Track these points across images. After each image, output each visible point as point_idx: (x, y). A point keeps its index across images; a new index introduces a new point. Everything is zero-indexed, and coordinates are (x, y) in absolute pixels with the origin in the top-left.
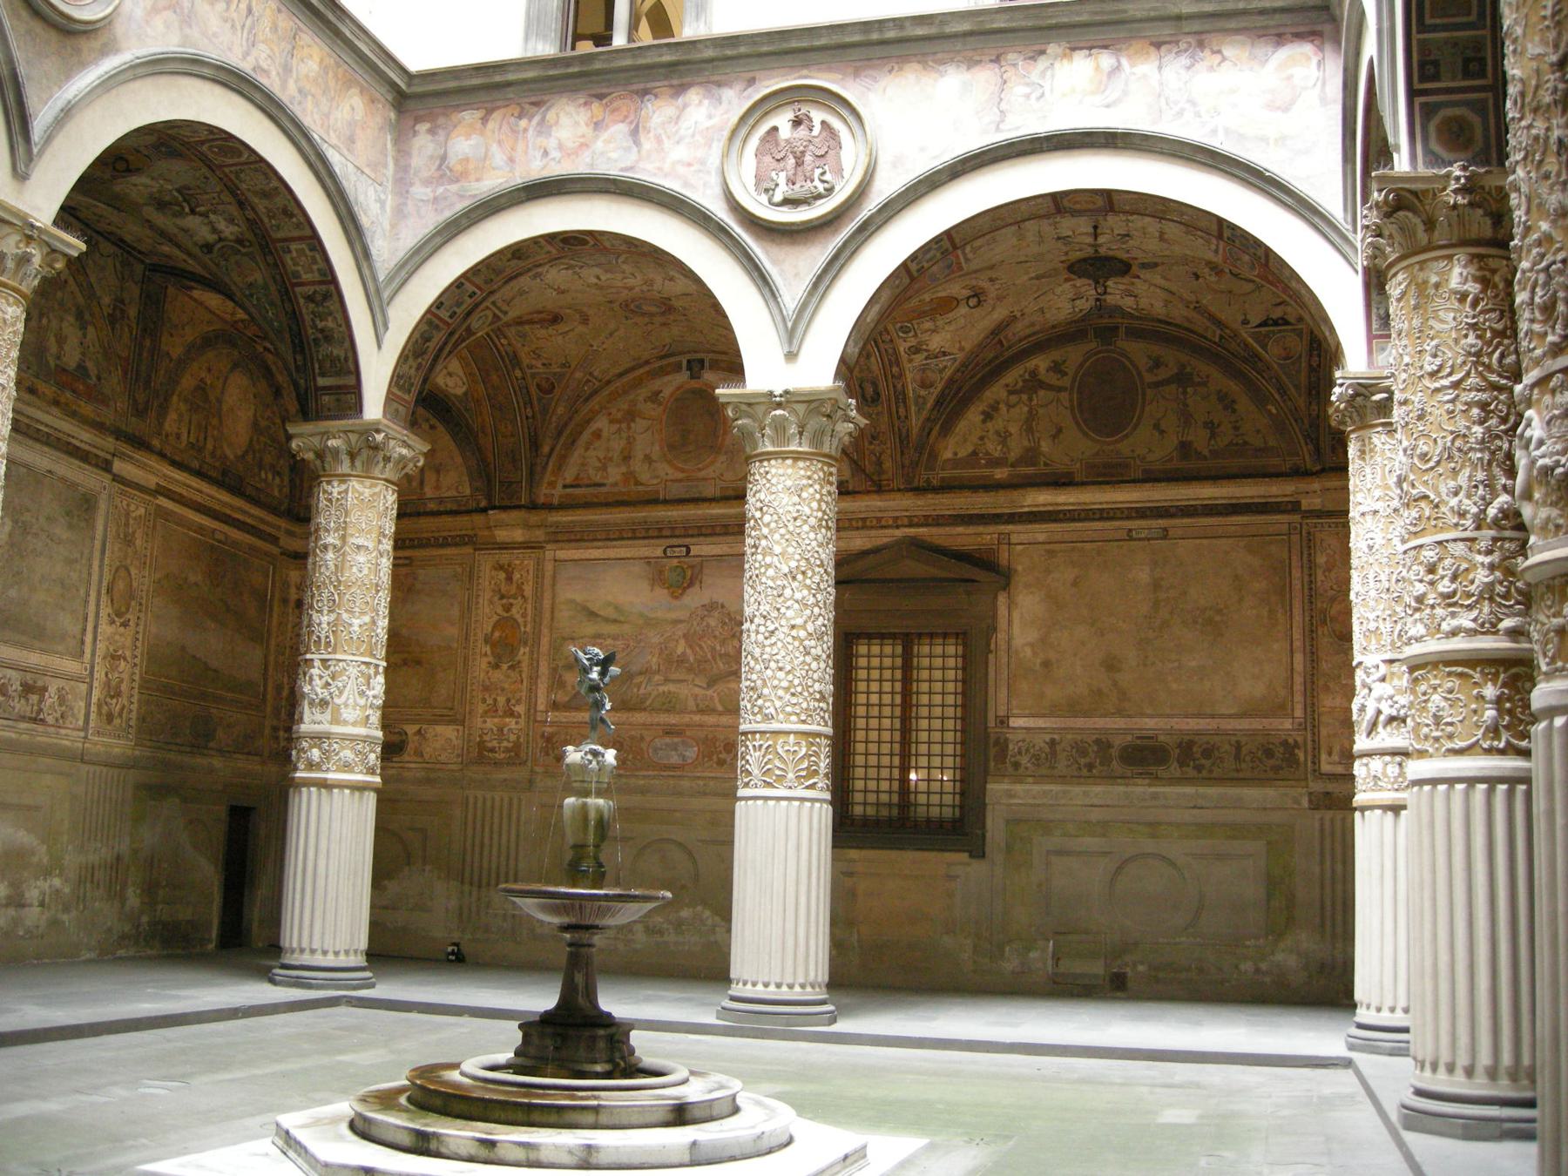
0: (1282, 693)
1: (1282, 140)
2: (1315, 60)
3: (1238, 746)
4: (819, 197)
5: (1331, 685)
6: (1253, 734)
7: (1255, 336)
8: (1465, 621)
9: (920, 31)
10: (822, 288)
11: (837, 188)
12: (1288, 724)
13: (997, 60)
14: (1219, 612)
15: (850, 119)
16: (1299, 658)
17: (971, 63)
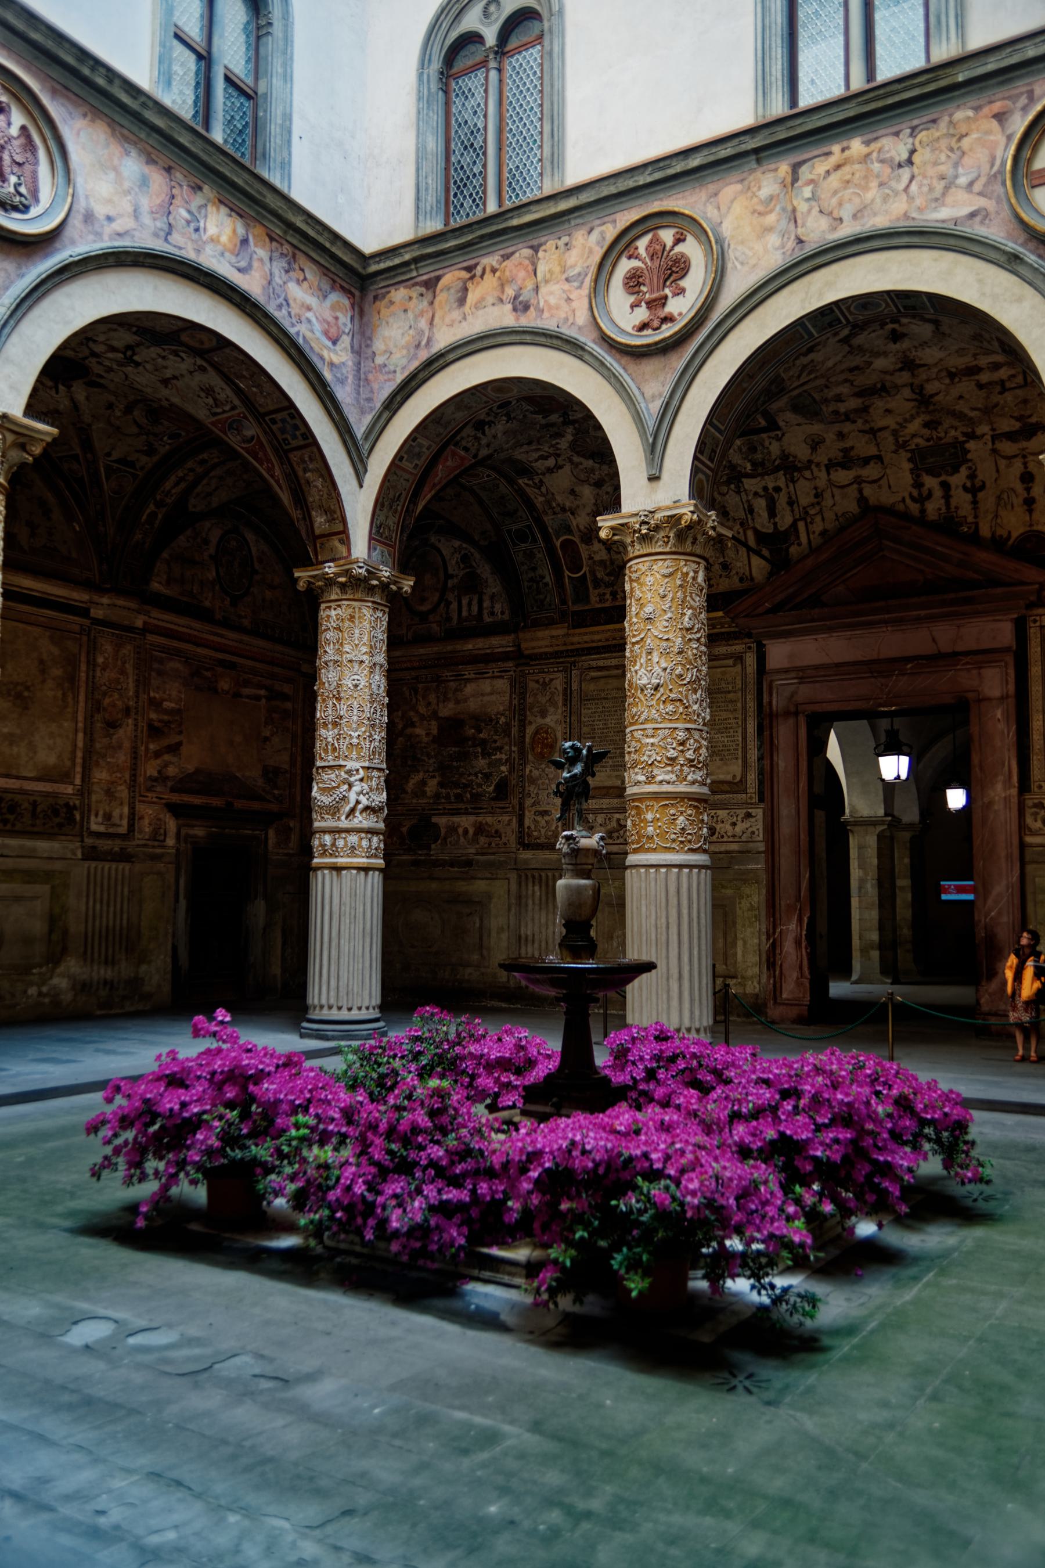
0: (68, 763)
1: (332, 364)
2: (349, 315)
3: (35, 804)
4: (15, 208)
5: (101, 761)
6: (47, 795)
8: (698, 776)
9: (125, 98)
10: (19, 313)
11: (34, 212)
12: (70, 790)
13: (168, 170)
14: (27, 688)
15: (52, 143)
16: (80, 736)
17: (151, 161)
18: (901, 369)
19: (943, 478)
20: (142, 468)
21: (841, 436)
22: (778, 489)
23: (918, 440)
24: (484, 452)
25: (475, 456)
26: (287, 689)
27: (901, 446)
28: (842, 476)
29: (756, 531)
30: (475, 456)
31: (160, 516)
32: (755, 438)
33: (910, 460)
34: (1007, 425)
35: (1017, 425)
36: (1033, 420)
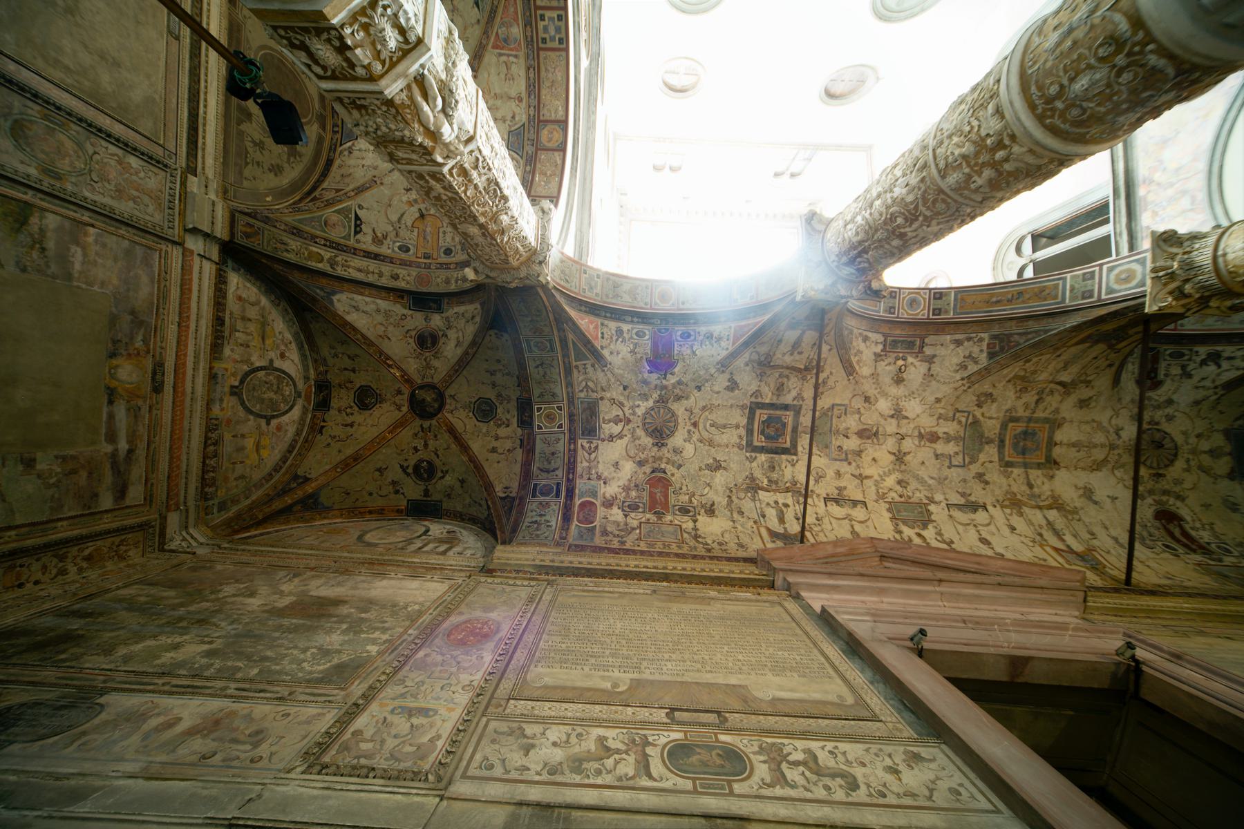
7: (348, 209)
18: (892, 417)
19: (917, 530)
20: (358, 241)
21: (838, 474)
22: (786, 506)
23: (893, 494)
24: (606, 353)
25: (602, 348)
26: (135, 493)
27: (881, 497)
28: (834, 509)
29: (768, 530)
30: (602, 348)
31: (320, 265)
32: (776, 457)
33: (889, 510)
34: (956, 499)
35: (962, 501)
36: (972, 498)
